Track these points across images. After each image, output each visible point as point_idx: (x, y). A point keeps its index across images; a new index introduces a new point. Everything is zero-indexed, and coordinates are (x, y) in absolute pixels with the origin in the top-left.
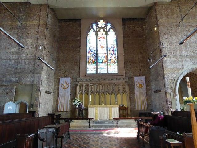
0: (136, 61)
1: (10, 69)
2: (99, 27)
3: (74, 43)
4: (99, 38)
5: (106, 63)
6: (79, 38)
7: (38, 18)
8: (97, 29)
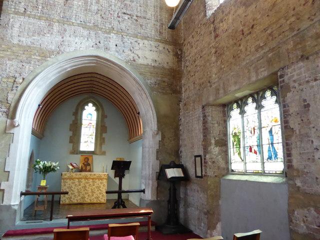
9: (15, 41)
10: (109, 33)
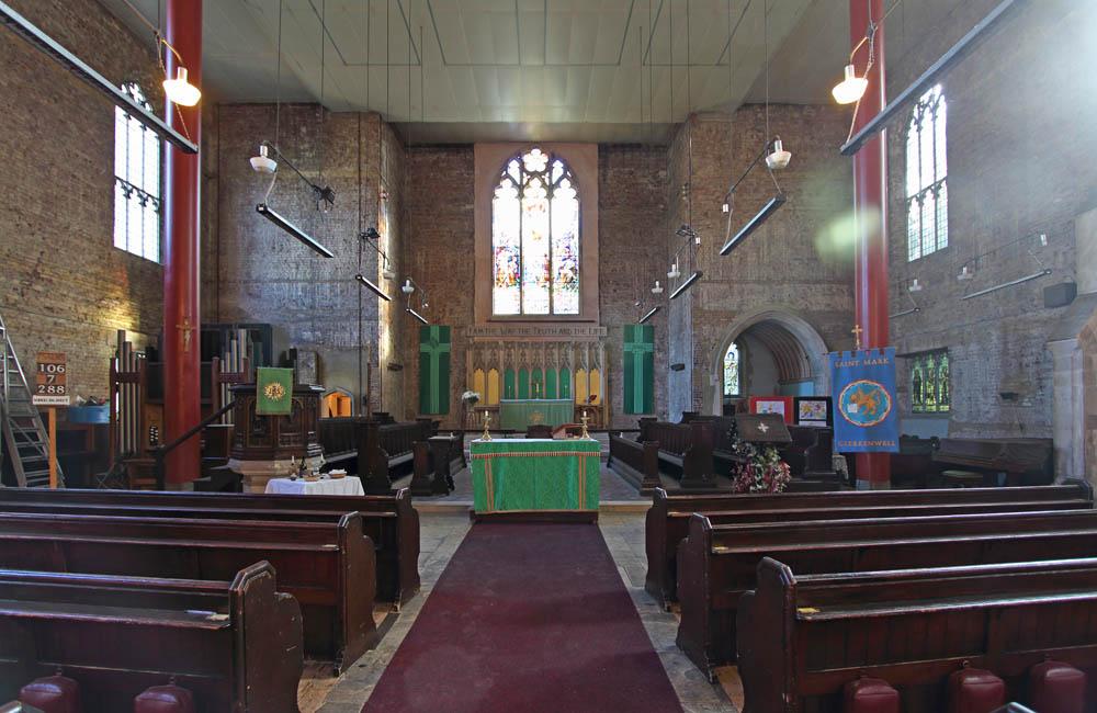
0: (632, 280)
1: (295, 308)
2: (528, 173)
3: (456, 222)
4: (530, 209)
5: (548, 284)
6: (468, 207)
7: (356, 159)
8: (521, 180)
9: (706, 308)
10: (781, 284)
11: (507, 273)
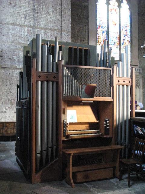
3: (80, 10)
4: (111, 10)
6: (86, 4)
11: (102, 38)
